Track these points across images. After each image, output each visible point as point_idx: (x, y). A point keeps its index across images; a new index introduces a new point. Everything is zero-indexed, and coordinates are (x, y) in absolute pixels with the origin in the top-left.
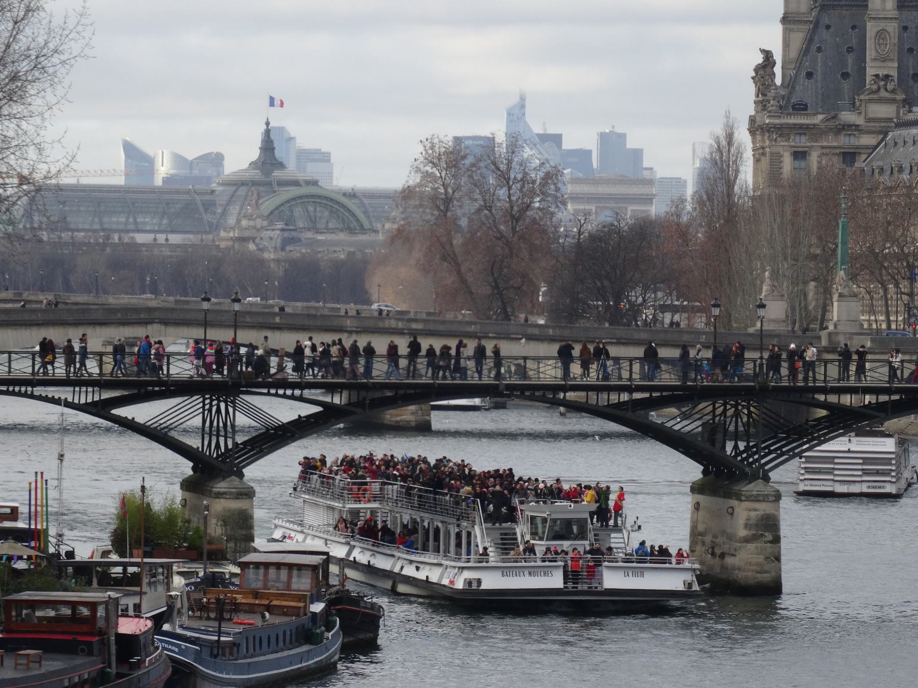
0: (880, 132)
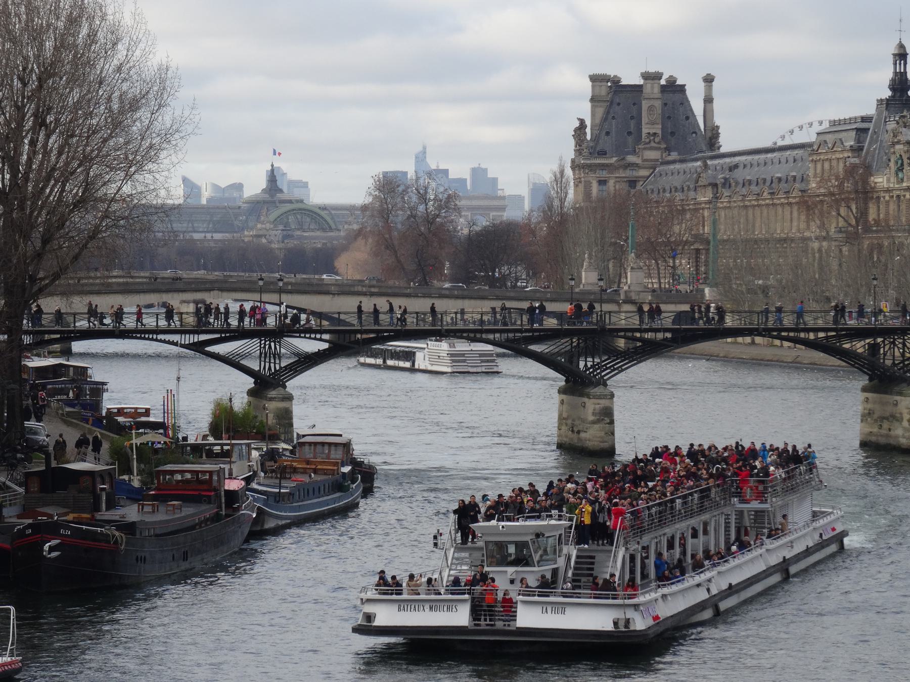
0: (651, 168)
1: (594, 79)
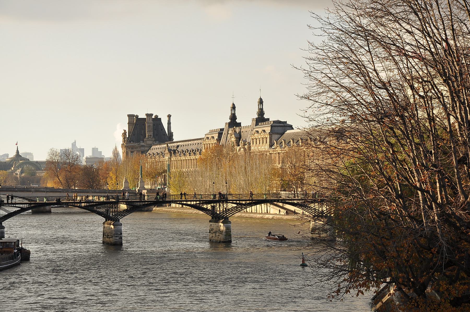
1: (129, 116)
